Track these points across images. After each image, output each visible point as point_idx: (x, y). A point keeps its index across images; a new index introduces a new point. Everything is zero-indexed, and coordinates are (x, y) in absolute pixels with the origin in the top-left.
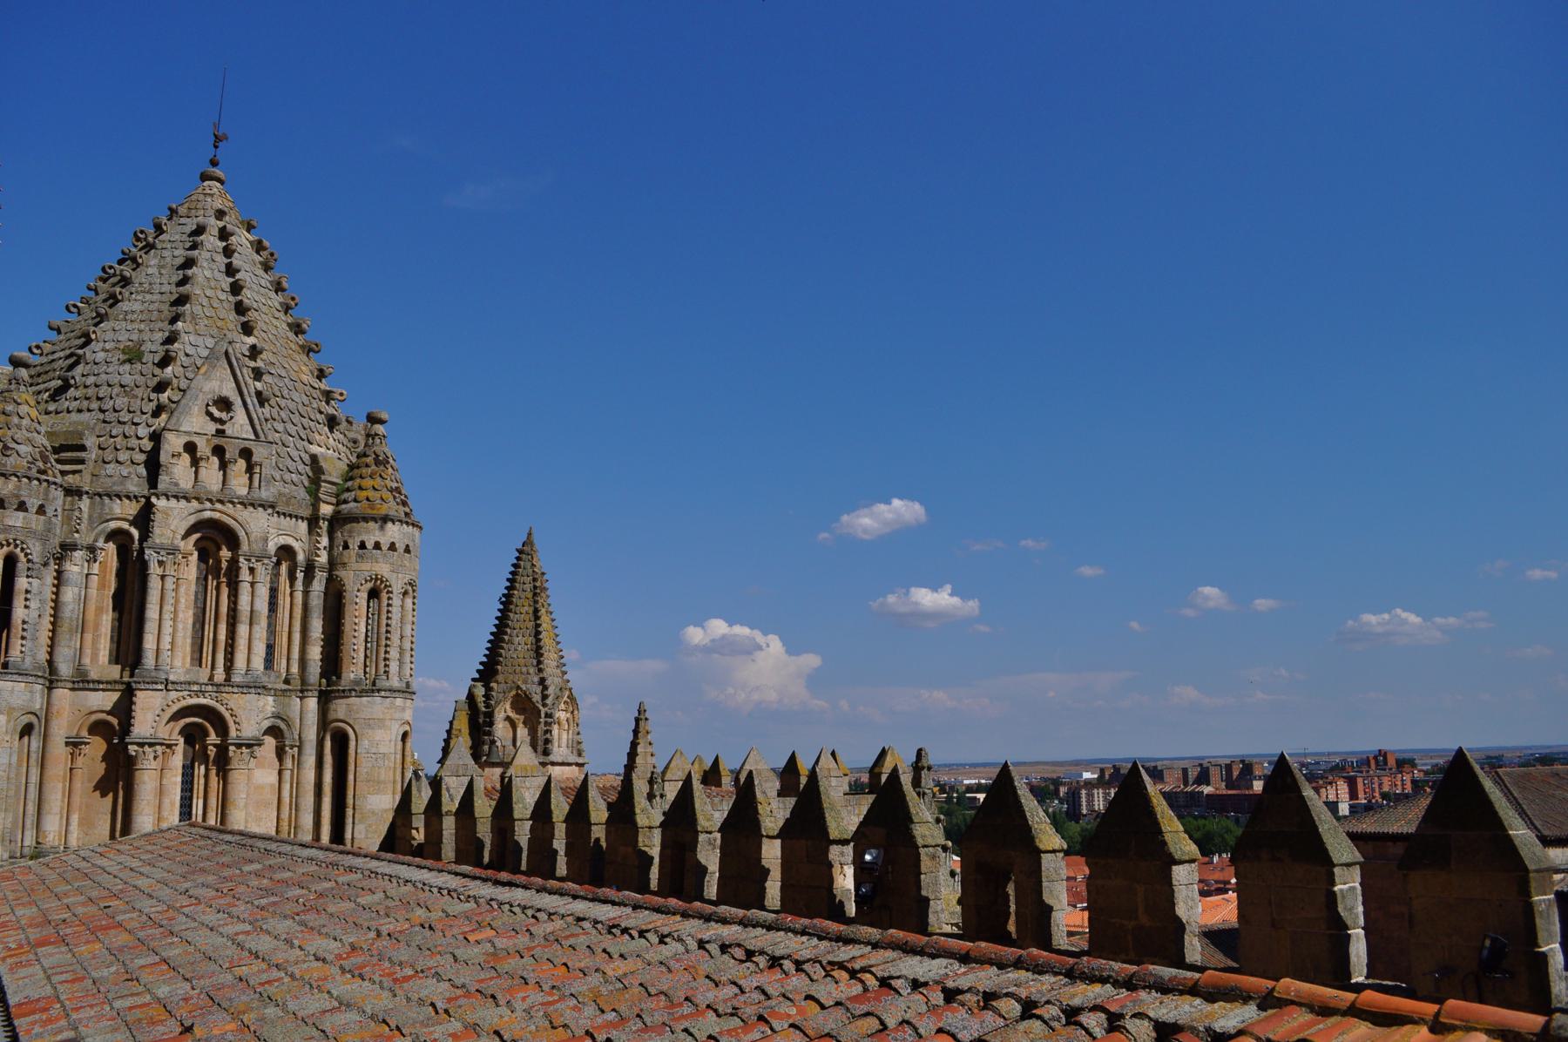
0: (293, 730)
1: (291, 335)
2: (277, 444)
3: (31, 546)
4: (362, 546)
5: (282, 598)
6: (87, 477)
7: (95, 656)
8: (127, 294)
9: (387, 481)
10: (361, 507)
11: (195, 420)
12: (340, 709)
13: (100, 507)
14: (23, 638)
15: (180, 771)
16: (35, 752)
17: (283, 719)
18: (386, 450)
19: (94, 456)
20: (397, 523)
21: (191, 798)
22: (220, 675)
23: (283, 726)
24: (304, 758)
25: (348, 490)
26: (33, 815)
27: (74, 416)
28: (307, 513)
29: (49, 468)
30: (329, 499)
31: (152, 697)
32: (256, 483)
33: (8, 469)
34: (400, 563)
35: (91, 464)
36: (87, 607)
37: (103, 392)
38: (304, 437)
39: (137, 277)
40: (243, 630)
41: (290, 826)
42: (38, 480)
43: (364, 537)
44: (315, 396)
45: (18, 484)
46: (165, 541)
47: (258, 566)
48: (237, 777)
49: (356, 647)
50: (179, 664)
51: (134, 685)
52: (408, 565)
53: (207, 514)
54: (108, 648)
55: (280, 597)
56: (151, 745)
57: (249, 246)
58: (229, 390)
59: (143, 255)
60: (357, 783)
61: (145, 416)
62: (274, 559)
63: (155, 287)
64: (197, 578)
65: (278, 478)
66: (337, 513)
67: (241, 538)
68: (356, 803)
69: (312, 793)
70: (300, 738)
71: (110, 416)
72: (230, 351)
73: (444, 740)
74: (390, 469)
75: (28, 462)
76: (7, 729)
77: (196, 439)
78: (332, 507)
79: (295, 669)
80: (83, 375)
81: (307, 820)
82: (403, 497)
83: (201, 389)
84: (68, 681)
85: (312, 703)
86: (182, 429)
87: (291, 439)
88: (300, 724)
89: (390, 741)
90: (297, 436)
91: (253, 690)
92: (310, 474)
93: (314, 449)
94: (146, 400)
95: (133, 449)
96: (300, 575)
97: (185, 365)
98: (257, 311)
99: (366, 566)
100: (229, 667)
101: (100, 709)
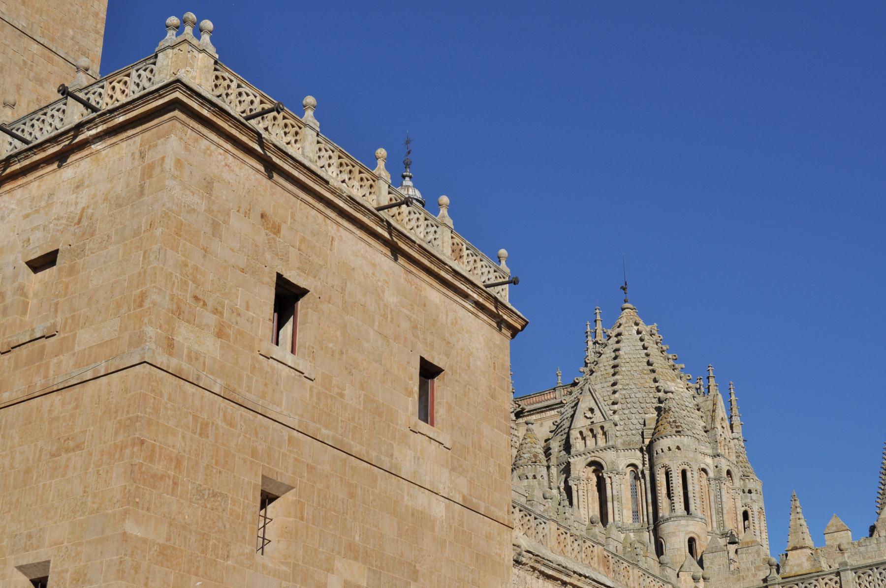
19: (556, 450)
34: (673, 455)
40: (610, 505)
52: (679, 455)
53: (590, 459)
72: (590, 387)
74: (671, 413)
82: (679, 424)
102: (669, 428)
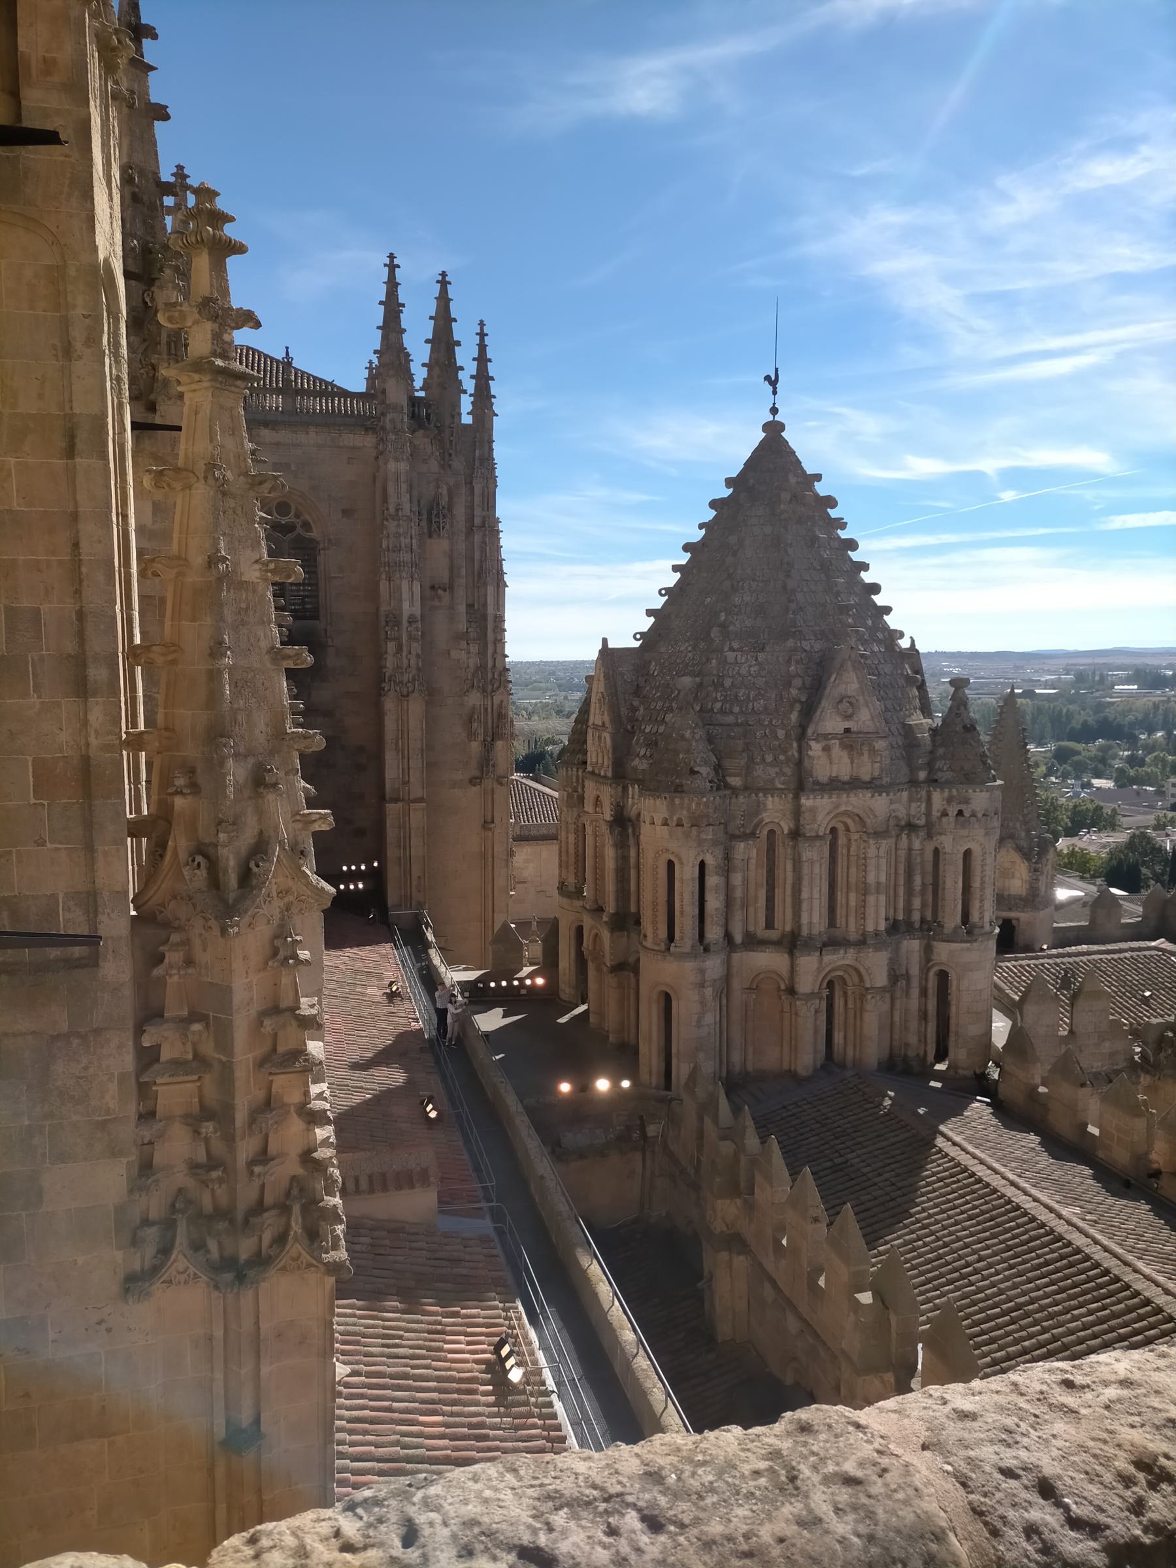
4: (960, 813)
12: (943, 951)
40: (871, 900)
53: (843, 808)
70: (907, 971)
81: (913, 1039)
99: (964, 832)
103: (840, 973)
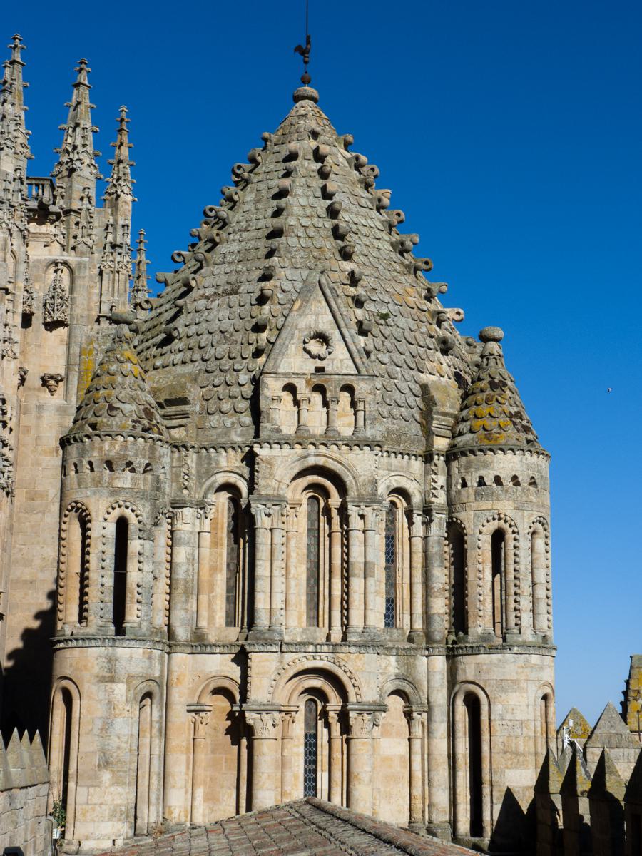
0: (421, 694)
1: (396, 256)
2: (383, 377)
3: (140, 507)
4: (481, 482)
5: (400, 546)
6: (193, 432)
7: (211, 619)
8: (224, 236)
9: (504, 407)
10: (477, 437)
11: (292, 360)
12: (469, 666)
13: (206, 461)
14: (138, 602)
15: (302, 740)
16: (157, 722)
17: (411, 683)
18: (502, 371)
19: (198, 409)
20: (518, 452)
21: (315, 771)
22: (337, 636)
23: (408, 689)
24: (435, 726)
25: (463, 420)
26: (158, 789)
27: (180, 369)
28: (420, 449)
29: (154, 425)
30: (443, 432)
31: (267, 660)
32: (361, 423)
33: (114, 429)
34: (525, 499)
35: (196, 418)
36: (201, 567)
37: (204, 340)
38: (413, 366)
39: (234, 217)
40: (357, 583)
41: (423, 803)
42: (143, 438)
43: (483, 472)
44: (424, 319)
45: (124, 444)
46: (271, 493)
47: (368, 512)
48: (360, 747)
49: (481, 598)
50: (294, 622)
51: (247, 648)
52: (534, 500)
53: (312, 461)
54: (224, 609)
55: (398, 545)
56: (268, 712)
57: (347, 165)
58: (325, 323)
59: (239, 192)
60: (493, 755)
61: (245, 361)
62: (387, 503)
63: (251, 223)
64: (309, 530)
65: (385, 414)
66: (453, 446)
67: (348, 483)
68: (493, 779)
69: (446, 766)
71: (212, 365)
72: (323, 281)
73: (622, 703)
74: (508, 392)
75: (133, 421)
76: (127, 696)
77: (295, 381)
78: (448, 440)
79: (419, 625)
80: (186, 326)
81: (442, 798)
82: (524, 423)
83: (297, 325)
84: (186, 645)
85: (440, 663)
86: (280, 370)
87: (398, 369)
88: (428, 687)
89: (528, 706)
90: (405, 366)
91: (371, 650)
92: (422, 406)
93: (425, 378)
94: (246, 344)
95: (236, 398)
96: (418, 520)
97: (282, 303)
98: (357, 234)
99: (486, 505)
100: (346, 626)
101: (222, 674)
102: (511, 431)
103: (317, 682)
